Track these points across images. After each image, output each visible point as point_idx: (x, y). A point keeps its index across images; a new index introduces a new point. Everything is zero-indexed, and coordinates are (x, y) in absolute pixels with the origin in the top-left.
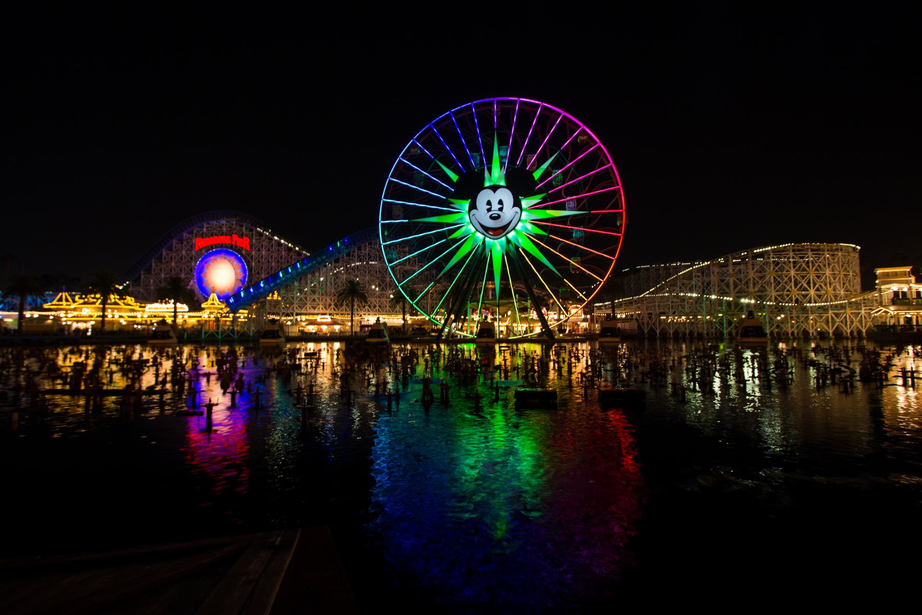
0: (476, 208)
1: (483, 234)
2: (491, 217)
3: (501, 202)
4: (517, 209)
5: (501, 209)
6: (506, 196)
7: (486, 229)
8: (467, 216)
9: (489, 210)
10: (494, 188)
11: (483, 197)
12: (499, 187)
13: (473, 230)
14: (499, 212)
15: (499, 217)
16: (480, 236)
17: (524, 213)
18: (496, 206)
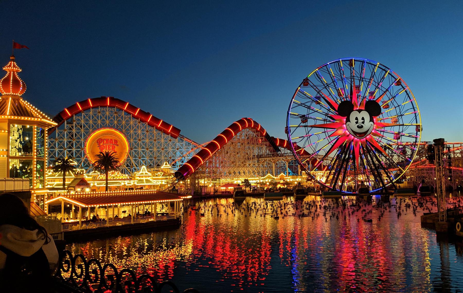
0: (350, 121)
1: (354, 136)
2: (358, 127)
3: (363, 119)
4: (372, 123)
5: (363, 123)
6: (366, 115)
7: (355, 133)
8: (345, 126)
9: (357, 123)
10: (360, 111)
11: (354, 115)
12: (362, 110)
13: (348, 133)
14: (362, 124)
15: (362, 127)
16: (353, 137)
17: (375, 125)
18: (360, 121)
